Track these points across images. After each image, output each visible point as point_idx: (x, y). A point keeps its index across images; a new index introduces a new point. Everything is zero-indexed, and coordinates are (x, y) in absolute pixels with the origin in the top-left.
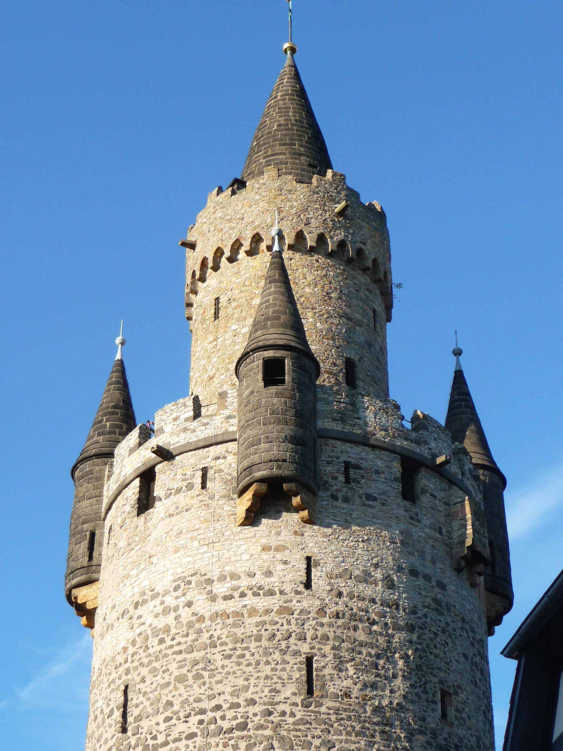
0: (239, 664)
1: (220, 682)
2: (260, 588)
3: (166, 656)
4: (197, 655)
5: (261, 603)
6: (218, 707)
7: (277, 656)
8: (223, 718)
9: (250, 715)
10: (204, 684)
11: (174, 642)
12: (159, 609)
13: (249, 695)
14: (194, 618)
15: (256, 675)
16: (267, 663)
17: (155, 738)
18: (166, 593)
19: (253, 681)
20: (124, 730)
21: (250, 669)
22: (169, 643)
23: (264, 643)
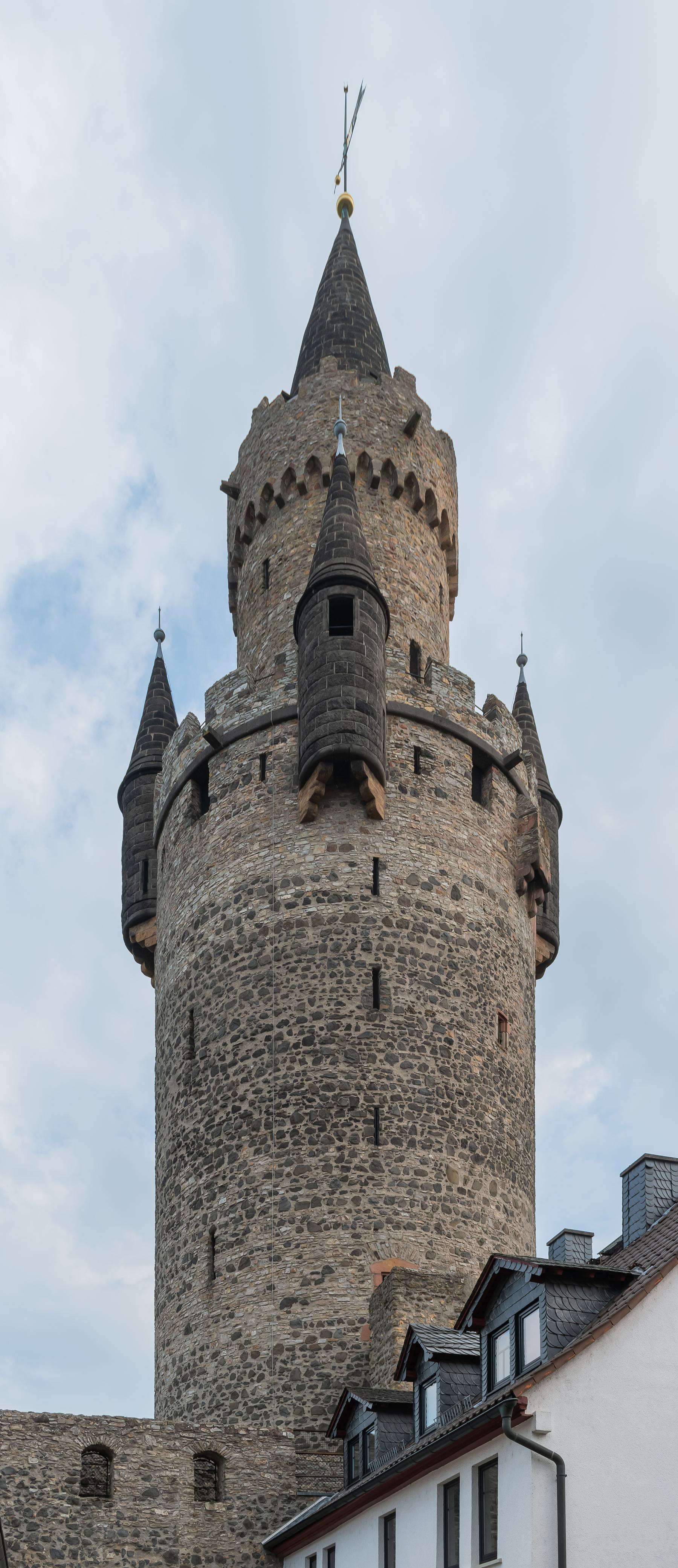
0: (304, 977)
1: (286, 996)
2: (325, 893)
3: (230, 974)
4: (263, 970)
5: (327, 910)
6: (285, 1023)
7: (342, 968)
8: (290, 1033)
9: (316, 1029)
10: (270, 999)
11: (238, 958)
12: (221, 924)
13: (314, 1009)
14: (257, 930)
15: (321, 988)
16: (332, 975)
17: (223, 1059)
18: (227, 906)
19: (318, 995)
20: (191, 1055)
21: (315, 982)
22: (232, 960)
23: (329, 954)
